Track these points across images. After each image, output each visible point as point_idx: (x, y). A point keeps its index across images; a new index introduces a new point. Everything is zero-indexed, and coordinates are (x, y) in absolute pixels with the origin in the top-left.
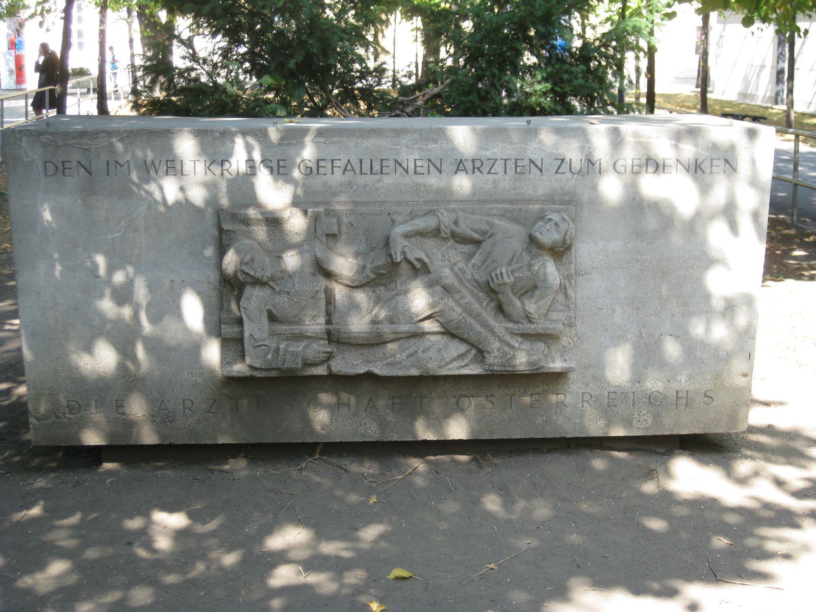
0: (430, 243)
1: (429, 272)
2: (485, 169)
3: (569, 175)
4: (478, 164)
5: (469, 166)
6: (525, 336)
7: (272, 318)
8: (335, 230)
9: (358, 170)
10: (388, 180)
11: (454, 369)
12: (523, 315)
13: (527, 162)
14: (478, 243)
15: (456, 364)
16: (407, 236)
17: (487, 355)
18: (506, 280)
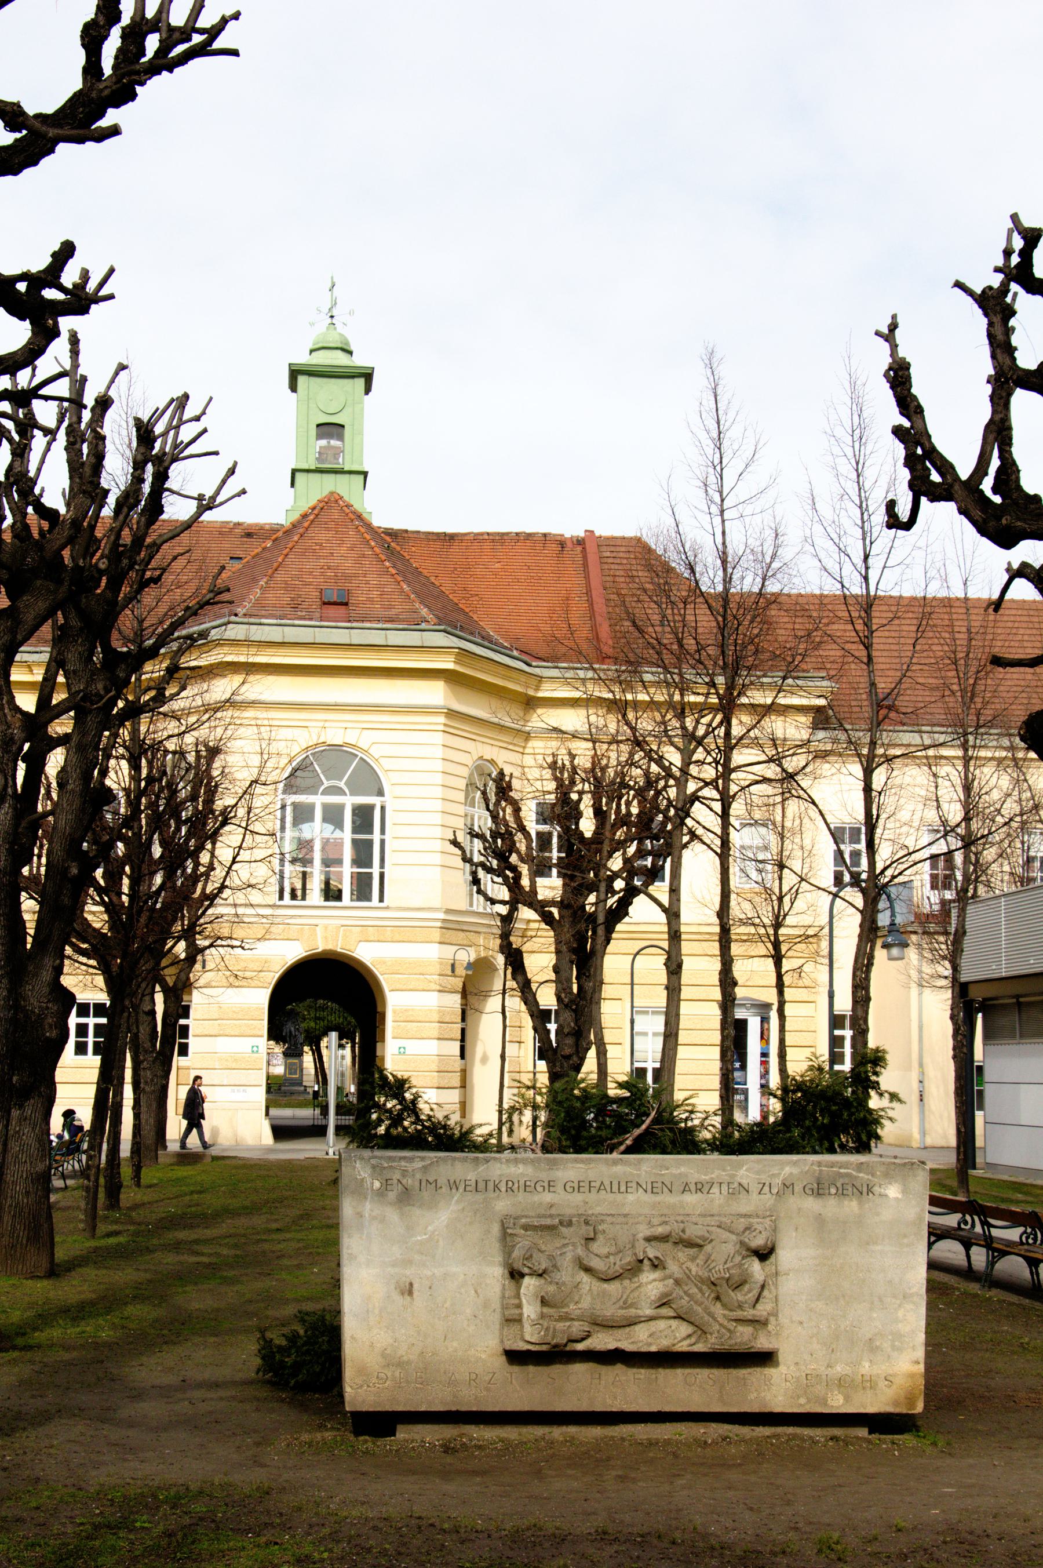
0: (668, 1246)
1: (664, 1268)
2: (705, 1190)
3: (769, 1195)
4: (700, 1186)
5: (693, 1187)
6: (737, 1320)
7: (544, 1302)
8: (592, 1235)
9: (609, 1190)
10: (631, 1198)
11: (683, 1347)
12: (736, 1304)
13: (736, 1185)
14: (701, 1246)
15: (688, 1342)
16: (648, 1239)
17: (709, 1336)
18: (723, 1274)
